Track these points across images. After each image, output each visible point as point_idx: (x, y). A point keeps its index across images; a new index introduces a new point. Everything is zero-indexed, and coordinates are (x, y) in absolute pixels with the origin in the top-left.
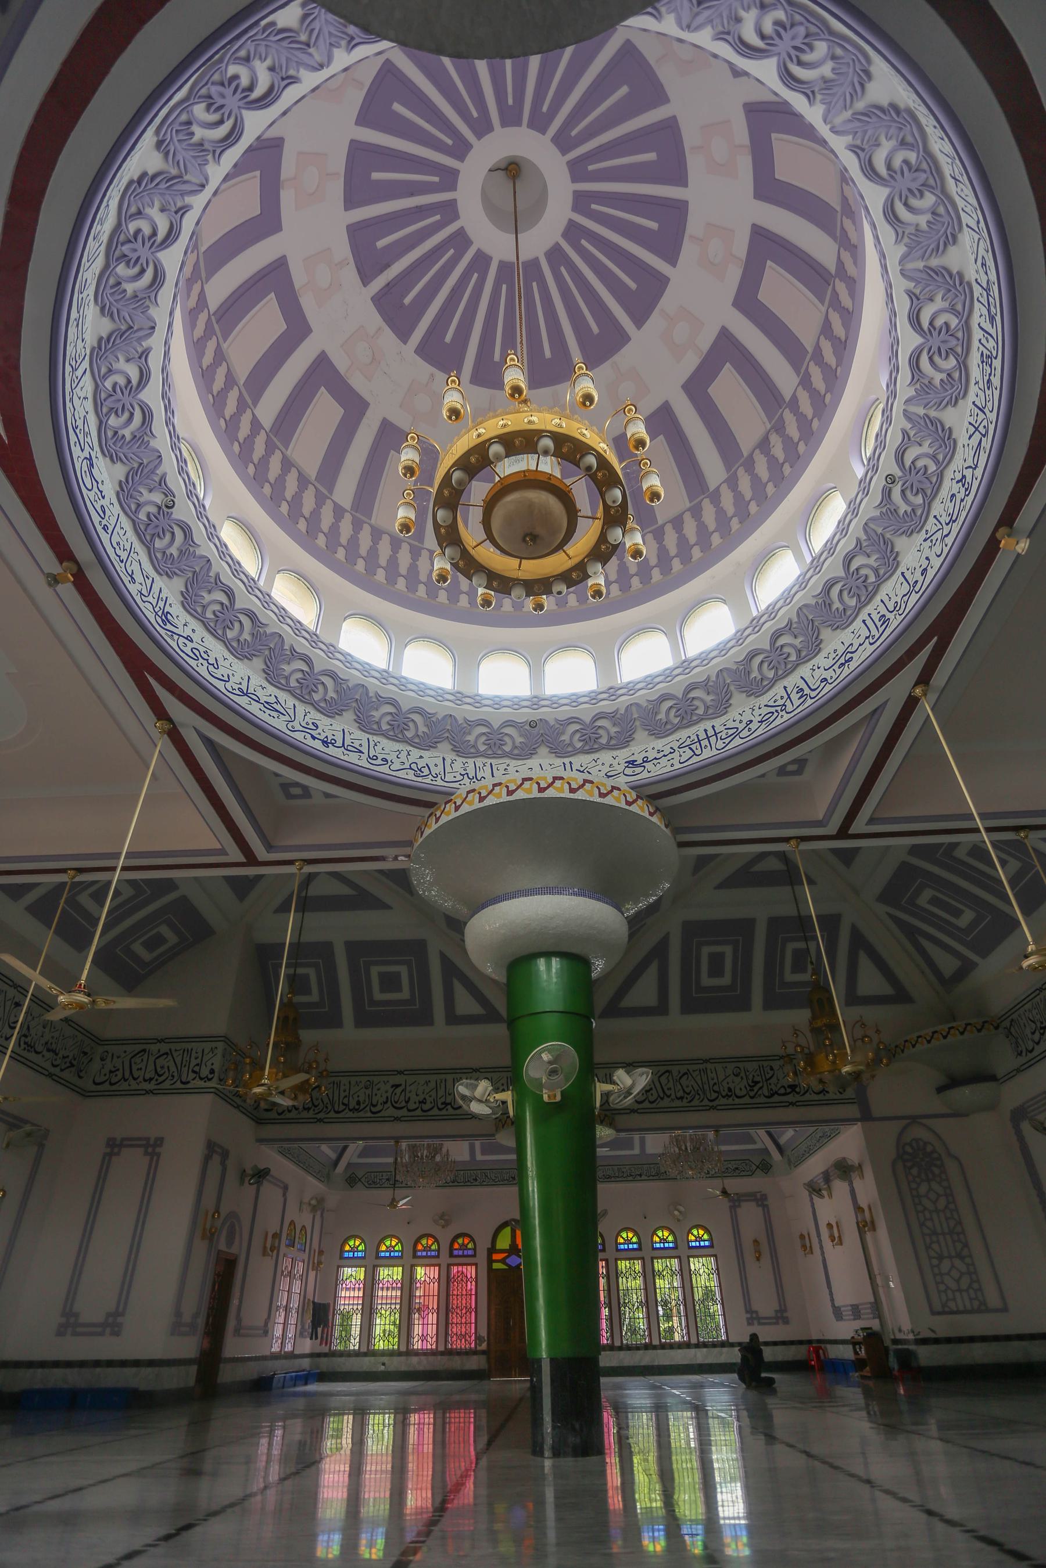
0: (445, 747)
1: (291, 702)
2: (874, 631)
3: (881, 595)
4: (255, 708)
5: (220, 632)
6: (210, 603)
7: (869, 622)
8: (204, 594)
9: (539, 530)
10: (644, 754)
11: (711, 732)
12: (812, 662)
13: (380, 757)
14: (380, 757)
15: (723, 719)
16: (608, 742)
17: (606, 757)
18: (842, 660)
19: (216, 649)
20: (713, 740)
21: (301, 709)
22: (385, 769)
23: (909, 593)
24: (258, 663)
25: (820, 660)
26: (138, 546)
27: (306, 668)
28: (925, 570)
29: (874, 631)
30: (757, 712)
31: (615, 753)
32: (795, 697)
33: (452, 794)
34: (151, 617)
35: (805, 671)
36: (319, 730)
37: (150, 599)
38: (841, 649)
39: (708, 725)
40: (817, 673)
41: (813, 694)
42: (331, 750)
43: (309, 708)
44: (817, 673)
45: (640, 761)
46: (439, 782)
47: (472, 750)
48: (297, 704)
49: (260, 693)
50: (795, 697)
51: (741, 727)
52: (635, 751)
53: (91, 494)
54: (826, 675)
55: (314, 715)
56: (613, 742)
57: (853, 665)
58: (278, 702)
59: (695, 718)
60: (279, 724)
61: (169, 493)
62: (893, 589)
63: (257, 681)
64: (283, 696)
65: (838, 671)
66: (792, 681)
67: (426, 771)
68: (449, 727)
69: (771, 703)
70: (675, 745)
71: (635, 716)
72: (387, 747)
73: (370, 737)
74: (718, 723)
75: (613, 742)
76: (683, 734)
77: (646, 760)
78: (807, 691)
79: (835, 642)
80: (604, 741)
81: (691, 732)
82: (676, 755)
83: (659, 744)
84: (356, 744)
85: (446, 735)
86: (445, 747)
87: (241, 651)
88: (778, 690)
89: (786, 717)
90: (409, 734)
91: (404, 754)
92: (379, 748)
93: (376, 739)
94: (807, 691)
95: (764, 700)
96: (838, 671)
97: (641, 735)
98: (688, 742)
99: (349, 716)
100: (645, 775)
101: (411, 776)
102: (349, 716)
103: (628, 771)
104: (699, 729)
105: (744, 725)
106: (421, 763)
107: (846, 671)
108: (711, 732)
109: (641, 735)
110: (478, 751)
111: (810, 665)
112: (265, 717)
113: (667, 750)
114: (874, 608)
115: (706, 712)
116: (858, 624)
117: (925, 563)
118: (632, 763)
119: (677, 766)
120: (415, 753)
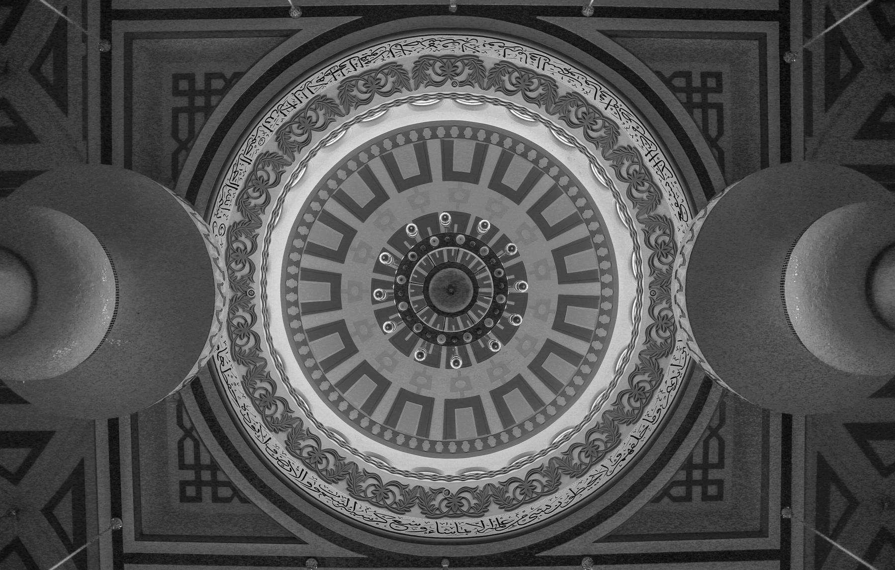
0: (663, 362)
1: (598, 467)
3: (522, 64)
4: (585, 493)
5: (534, 495)
6: (514, 494)
8: (507, 495)
9: (446, 284)
10: (674, 206)
11: (649, 157)
13: (655, 414)
14: (655, 414)
15: (640, 149)
16: (668, 235)
17: (679, 237)
18: (569, 75)
19: (542, 503)
20: (653, 154)
21: (605, 462)
22: (663, 412)
23: (508, 48)
24: (565, 479)
25: (579, 89)
26: (457, 520)
27: (579, 449)
28: (490, 44)
30: (627, 125)
31: (676, 230)
32: (607, 100)
33: (694, 362)
34: (495, 532)
35: (590, 98)
36: (623, 453)
37: (486, 527)
39: (646, 159)
41: (598, 88)
42: (636, 450)
43: (608, 456)
44: (587, 89)
45: (678, 209)
46: (683, 372)
47: (669, 341)
48: (602, 463)
49: (581, 486)
50: (607, 100)
51: (639, 135)
52: (673, 214)
53: (410, 529)
54: (583, 82)
55: (613, 455)
56: (668, 231)
57: (568, 67)
58: (593, 476)
59: (643, 171)
60: (604, 479)
61: (440, 491)
62: (516, 58)
63: (575, 484)
64: (592, 472)
65: (577, 75)
67: (674, 380)
68: (648, 357)
69: (617, 116)
70: (664, 182)
71: (646, 216)
72: (651, 409)
73: (643, 417)
74: (643, 152)
75: (668, 231)
76: (657, 178)
77: (677, 204)
78: (599, 93)
79: (565, 85)
80: (667, 239)
81: (653, 171)
82: (669, 180)
83: (666, 195)
84: (642, 429)
85: (653, 359)
86: (663, 362)
87: (553, 487)
88: (609, 113)
89: (620, 103)
90: (648, 387)
91: (661, 396)
92: (651, 413)
93: (645, 414)
94: (599, 93)
95: (618, 121)
96: (577, 75)
97: (661, 210)
98: (659, 173)
99: (623, 429)
100: (685, 203)
101: (673, 393)
102: (623, 429)
103: (685, 216)
104: (650, 165)
105: (637, 133)
106: (669, 384)
108: (649, 157)
109: (661, 210)
110: (670, 337)
111: (585, 96)
112: (595, 488)
113: (668, 188)
114: (532, 65)
115: (637, 163)
116: (547, 72)
117: (488, 46)
118: (680, 214)
119: (674, 179)
120: (663, 387)
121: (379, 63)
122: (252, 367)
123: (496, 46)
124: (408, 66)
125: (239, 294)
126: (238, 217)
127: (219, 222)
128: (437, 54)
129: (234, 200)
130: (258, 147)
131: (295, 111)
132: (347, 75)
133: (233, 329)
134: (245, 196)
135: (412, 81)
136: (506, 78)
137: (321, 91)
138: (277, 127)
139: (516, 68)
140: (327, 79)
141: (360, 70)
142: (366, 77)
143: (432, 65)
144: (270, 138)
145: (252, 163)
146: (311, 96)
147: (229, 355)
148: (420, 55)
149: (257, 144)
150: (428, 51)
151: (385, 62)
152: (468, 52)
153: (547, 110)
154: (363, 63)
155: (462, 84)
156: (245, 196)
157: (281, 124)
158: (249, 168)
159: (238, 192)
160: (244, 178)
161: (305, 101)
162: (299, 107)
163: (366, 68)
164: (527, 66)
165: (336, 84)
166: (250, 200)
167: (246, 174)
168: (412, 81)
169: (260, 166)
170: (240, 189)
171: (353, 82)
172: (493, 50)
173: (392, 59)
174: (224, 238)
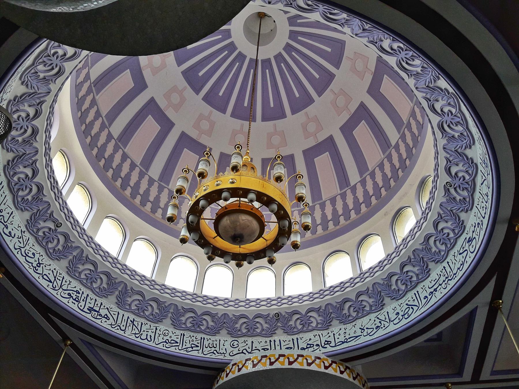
121: (75, 284)
122: (332, 315)
125: (279, 324)
126: (224, 332)
127: (229, 349)
130: (170, 335)
131: (137, 319)
133: (305, 329)
134: (208, 330)
137: (115, 308)
138: (153, 325)
140: (103, 312)
141: (87, 292)
142: (89, 285)
144: (162, 327)
146: (121, 312)
147: (325, 333)
148: (51, 262)
149: (168, 337)
150: (46, 260)
151: (71, 280)
152: (27, 235)
154: (80, 295)
156: (208, 330)
157: (149, 323)
158: (187, 334)
159: (206, 337)
160: (195, 335)
161: (127, 314)
162: (132, 317)
163: (83, 289)
165: (104, 301)
166: (210, 326)
167: (192, 334)
169: (183, 326)
170: (203, 336)
171: (98, 290)
173: (67, 278)
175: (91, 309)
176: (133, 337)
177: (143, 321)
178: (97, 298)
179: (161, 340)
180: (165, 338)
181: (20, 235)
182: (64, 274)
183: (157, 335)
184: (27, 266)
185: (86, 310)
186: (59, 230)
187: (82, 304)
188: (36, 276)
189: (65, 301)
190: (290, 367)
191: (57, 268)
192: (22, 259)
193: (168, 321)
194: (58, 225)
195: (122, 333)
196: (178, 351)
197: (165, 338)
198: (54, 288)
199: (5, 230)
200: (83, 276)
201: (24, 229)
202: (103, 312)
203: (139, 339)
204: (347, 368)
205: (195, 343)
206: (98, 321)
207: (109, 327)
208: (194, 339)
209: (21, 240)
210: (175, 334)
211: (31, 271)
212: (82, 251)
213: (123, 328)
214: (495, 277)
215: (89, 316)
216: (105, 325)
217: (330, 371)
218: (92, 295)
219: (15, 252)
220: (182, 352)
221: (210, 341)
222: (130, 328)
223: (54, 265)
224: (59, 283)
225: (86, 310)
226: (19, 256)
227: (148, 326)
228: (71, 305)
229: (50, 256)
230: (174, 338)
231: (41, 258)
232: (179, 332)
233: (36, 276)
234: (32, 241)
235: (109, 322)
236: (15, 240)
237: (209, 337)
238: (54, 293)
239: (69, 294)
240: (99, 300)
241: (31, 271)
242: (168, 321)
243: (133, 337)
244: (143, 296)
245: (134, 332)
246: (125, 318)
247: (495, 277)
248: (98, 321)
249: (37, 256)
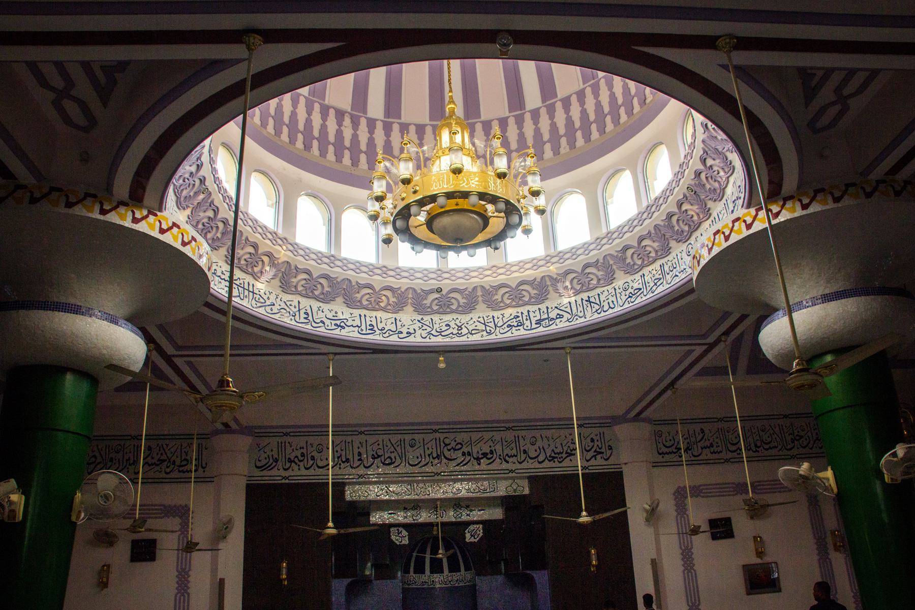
2: (363, 327)
3: (379, 314)
7: (363, 318)
12: (321, 304)
29: (363, 327)
35: (315, 304)
38: (340, 316)
40: (321, 315)
66: (305, 303)
69: (288, 303)
78: (310, 318)
88: (295, 299)
94: (310, 318)
95: (286, 297)
107: (337, 332)
116: (356, 312)
123: (405, 330)
124: (481, 306)
128: (455, 316)
129: (670, 258)
130: (631, 284)
131: (591, 294)
132: (536, 308)
135: (479, 293)
136: (392, 300)
138: (609, 288)
139: (384, 310)
140: (553, 315)
141: (524, 310)
143: (459, 306)
144: (619, 284)
145: (641, 273)
148: (471, 315)
150: (464, 318)
151: (502, 312)
152: (427, 318)
153: (350, 281)
154: (520, 318)
155: (431, 291)
157: (605, 289)
158: (646, 271)
163: (520, 310)
164: (374, 314)
165: (547, 303)
168: (479, 293)
172: (406, 327)
173: (496, 314)
174: (692, 240)
175: (539, 322)
176: (596, 316)
177: (598, 291)
178: (540, 306)
179: (624, 298)
180: (627, 293)
181: (420, 325)
182: (491, 314)
183: (618, 295)
184: (448, 340)
185: (534, 326)
186: (444, 292)
187: (527, 323)
188: (464, 338)
189: (509, 334)
190: (751, 231)
191: (481, 315)
192: (439, 339)
193: (619, 274)
194: (439, 290)
195: (583, 320)
196: (644, 298)
197: (627, 293)
198: (490, 333)
199: (401, 336)
200: (508, 302)
201: (419, 318)
202: (553, 315)
203: (603, 314)
204: (785, 200)
205: (657, 276)
206: (554, 327)
207: (568, 324)
208: (654, 272)
209: (425, 327)
210: (635, 281)
211: (457, 339)
212: (482, 287)
213: (582, 314)
214: (636, 48)
215: (541, 329)
216: (561, 325)
217: (758, 227)
218: (532, 308)
219: (427, 340)
220: (648, 296)
221: (670, 264)
222: (589, 309)
223: (475, 315)
224: (492, 325)
225: (534, 326)
226: (434, 339)
227: (606, 293)
228: (516, 333)
229: (464, 312)
230: (636, 286)
231: (458, 322)
232: (637, 276)
233: (464, 338)
234: (436, 318)
235: (564, 319)
236: (419, 332)
237: (666, 259)
238: (493, 336)
239: (509, 326)
240: (543, 307)
241: (457, 339)
242: (619, 274)
243: (596, 316)
244: (573, 271)
245: (594, 310)
246: (579, 302)
247: (636, 48)
248: (554, 327)
249: (452, 324)
